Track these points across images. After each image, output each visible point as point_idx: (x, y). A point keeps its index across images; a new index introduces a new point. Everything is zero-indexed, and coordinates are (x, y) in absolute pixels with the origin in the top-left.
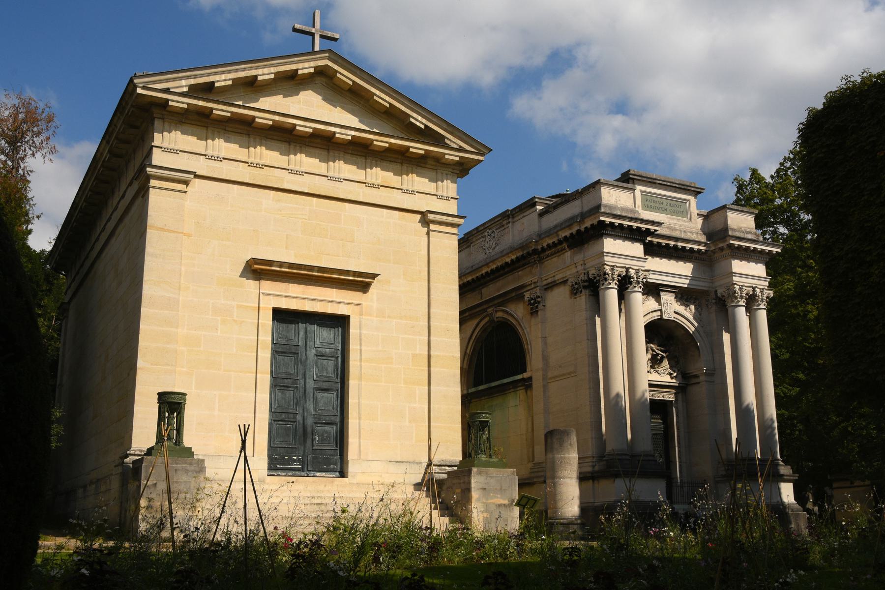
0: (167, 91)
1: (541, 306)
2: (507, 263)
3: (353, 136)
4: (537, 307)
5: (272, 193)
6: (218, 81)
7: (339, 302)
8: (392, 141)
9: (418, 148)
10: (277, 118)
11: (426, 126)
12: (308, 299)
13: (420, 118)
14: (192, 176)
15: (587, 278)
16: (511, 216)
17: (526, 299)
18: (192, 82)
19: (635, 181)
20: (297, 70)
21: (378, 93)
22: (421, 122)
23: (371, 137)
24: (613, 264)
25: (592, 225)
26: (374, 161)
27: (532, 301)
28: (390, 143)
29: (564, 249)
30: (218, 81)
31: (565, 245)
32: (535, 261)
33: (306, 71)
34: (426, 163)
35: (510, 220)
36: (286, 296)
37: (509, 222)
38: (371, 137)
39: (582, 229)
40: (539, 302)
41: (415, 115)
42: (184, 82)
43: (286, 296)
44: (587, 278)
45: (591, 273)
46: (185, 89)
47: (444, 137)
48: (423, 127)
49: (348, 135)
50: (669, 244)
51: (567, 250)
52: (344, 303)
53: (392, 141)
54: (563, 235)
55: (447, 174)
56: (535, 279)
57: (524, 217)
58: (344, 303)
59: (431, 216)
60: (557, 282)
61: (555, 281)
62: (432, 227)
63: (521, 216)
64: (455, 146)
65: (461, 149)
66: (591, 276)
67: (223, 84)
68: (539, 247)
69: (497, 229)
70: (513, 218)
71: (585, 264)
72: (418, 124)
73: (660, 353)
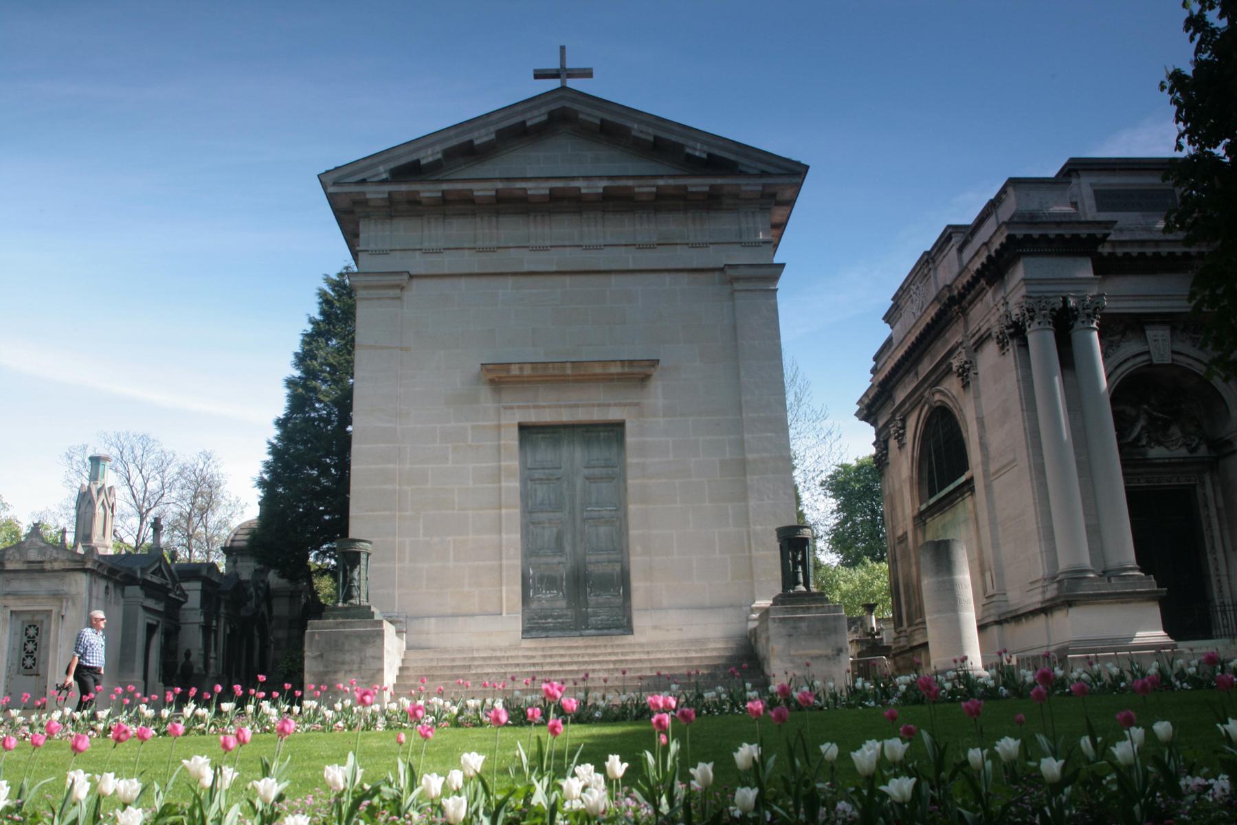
0: (363, 181)
1: (971, 374)
2: (928, 324)
4: (967, 376)
6: (423, 158)
8: (661, 182)
9: (699, 184)
10: (500, 185)
11: (710, 155)
13: (699, 146)
14: (406, 277)
15: (1010, 323)
16: (930, 261)
17: (954, 369)
18: (392, 165)
19: (1080, 172)
20: (524, 122)
21: (636, 126)
22: (701, 151)
23: (630, 183)
24: (1041, 294)
25: (1002, 245)
26: (645, 215)
27: (960, 371)
28: (658, 187)
29: (984, 289)
30: (423, 158)
31: (983, 282)
32: (957, 313)
33: (536, 121)
35: (931, 266)
37: (930, 269)
38: (630, 183)
39: (993, 254)
40: (969, 369)
41: (690, 143)
42: (381, 169)
44: (1010, 323)
45: (1013, 313)
46: (384, 176)
47: (734, 164)
48: (704, 156)
50: (1144, 254)
51: (987, 288)
53: (661, 182)
54: (975, 269)
55: (753, 213)
56: (959, 338)
57: (944, 257)
60: (984, 337)
61: (982, 336)
62: (737, 286)
63: (941, 257)
64: (756, 172)
66: (1014, 319)
67: (430, 159)
68: (956, 293)
69: (921, 283)
70: (934, 262)
71: (1007, 303)
72: (697, 154)
73: (1161, 415)
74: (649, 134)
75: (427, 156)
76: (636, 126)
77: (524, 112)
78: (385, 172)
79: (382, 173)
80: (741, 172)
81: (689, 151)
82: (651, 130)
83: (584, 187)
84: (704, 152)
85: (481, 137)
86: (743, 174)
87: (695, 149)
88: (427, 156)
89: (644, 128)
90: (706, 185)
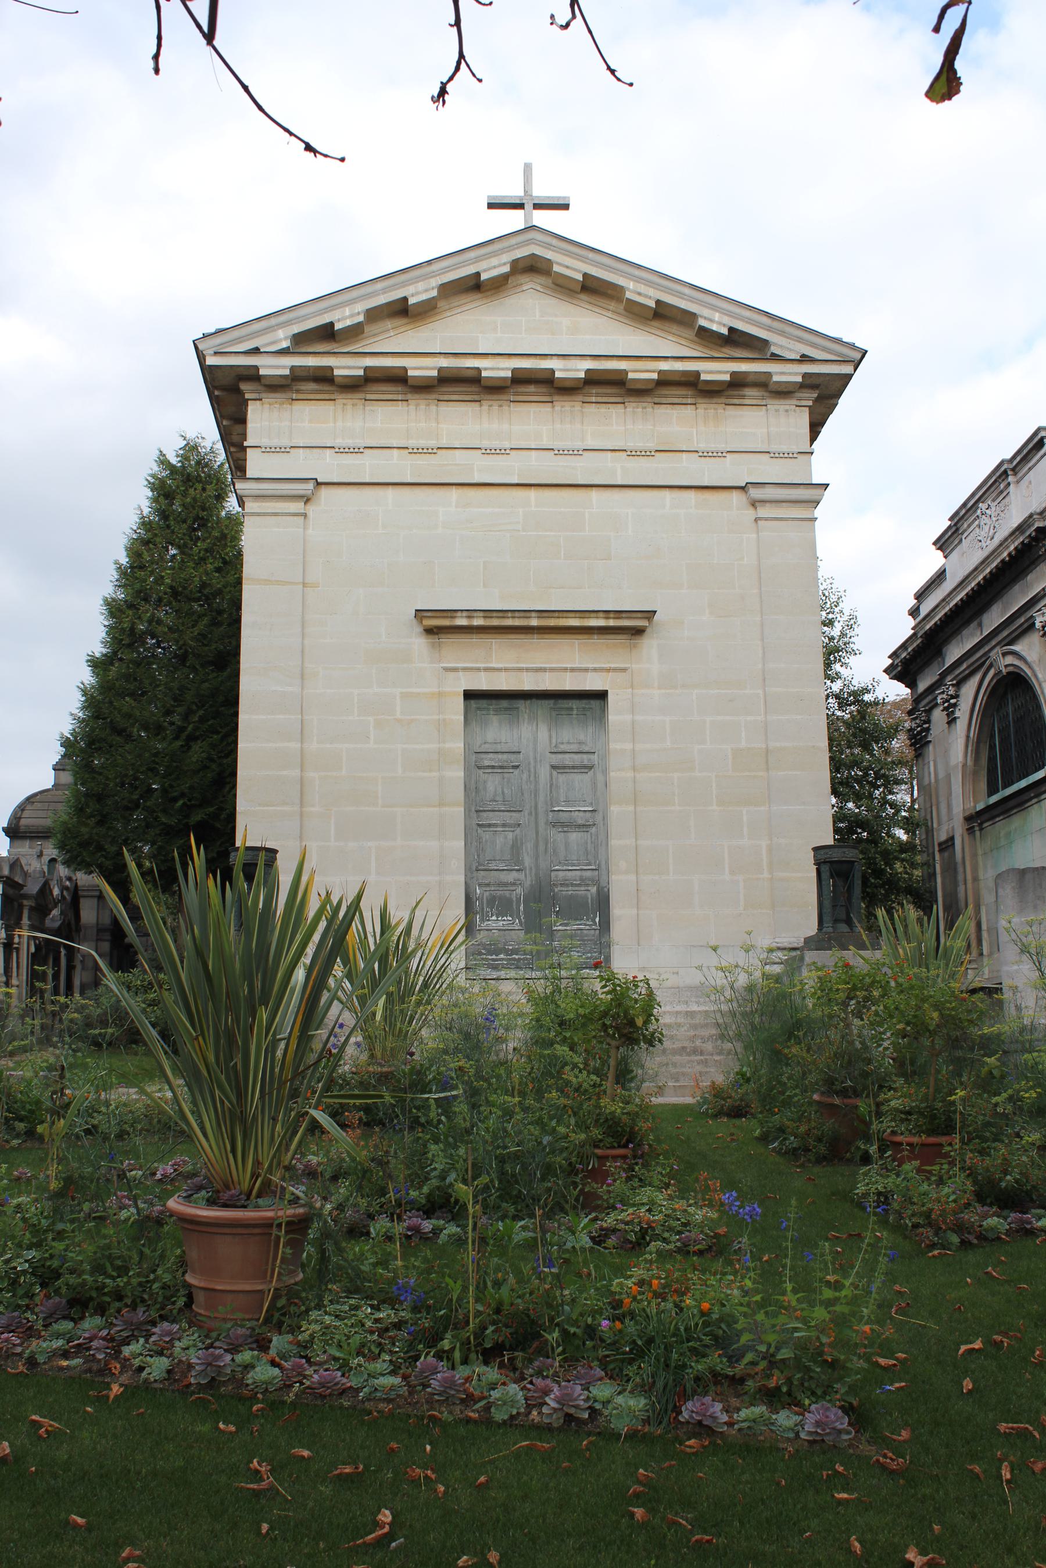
3: (588, 371)
5: (454, 492)
6: (339, 320)
7: (586, 670)
10: (444, 362)
12: (527, 670)
13: (717, 316)
20: (478, 274)
21: (631, 285)
22: (719, 323)
23: (622, 365)
34: (743, 397)
36: (486, 669)
43: (486, 669)
46: (285, 344)
49: (578, 370)
52: (595, 670)
55: (787, 411)
58: (595, 670)
59: (755, 493)
65: (805, 359)
72: (714, 327)
74: (648, 296)
75: (344, 318)
76: (631, 285)
77: (478, 260)
78: (286, 338)
79: (281, 340)
80: (773, 354)
81: (702, 322)
82: (651, 292)
83: (563, 370)
84: (724, 325)
85: (418, 293)
86: (776, 358)
87: (711, 320)
88: (344, 318)
89: (642, 288)
90: (726, 372)
